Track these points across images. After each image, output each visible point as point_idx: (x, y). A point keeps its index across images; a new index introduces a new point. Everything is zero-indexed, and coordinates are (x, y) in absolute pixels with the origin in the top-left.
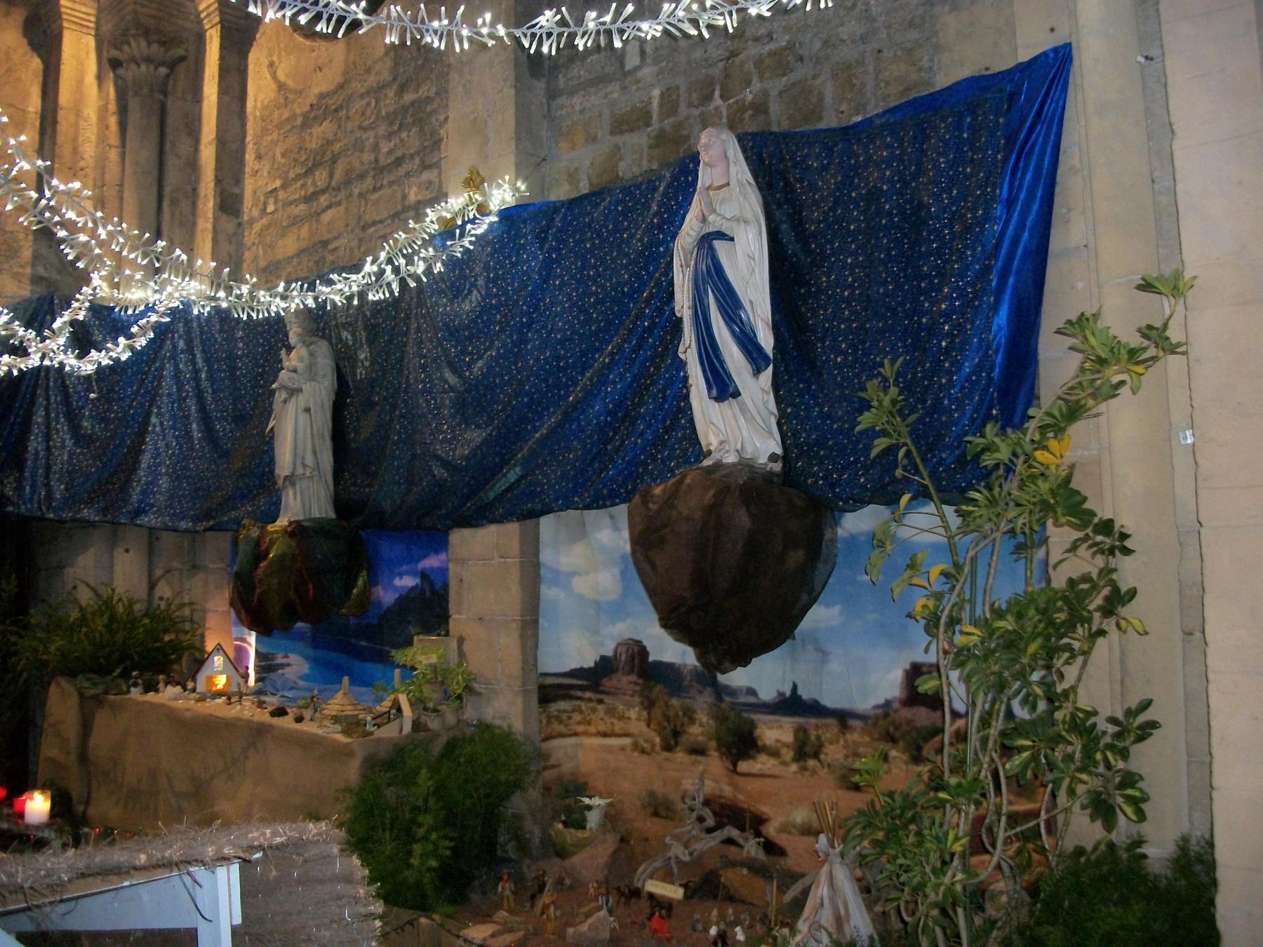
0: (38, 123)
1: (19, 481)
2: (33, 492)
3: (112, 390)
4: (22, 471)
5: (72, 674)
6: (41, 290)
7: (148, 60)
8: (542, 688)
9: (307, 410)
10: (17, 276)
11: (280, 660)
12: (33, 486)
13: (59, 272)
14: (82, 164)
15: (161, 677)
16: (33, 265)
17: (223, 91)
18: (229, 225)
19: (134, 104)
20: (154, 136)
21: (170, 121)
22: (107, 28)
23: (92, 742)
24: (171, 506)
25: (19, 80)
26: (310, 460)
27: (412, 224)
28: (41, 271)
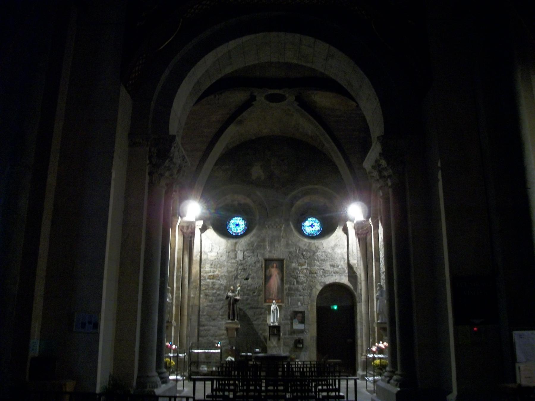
14: (354, 254)
18: (378, 264)
22: (356, 227)
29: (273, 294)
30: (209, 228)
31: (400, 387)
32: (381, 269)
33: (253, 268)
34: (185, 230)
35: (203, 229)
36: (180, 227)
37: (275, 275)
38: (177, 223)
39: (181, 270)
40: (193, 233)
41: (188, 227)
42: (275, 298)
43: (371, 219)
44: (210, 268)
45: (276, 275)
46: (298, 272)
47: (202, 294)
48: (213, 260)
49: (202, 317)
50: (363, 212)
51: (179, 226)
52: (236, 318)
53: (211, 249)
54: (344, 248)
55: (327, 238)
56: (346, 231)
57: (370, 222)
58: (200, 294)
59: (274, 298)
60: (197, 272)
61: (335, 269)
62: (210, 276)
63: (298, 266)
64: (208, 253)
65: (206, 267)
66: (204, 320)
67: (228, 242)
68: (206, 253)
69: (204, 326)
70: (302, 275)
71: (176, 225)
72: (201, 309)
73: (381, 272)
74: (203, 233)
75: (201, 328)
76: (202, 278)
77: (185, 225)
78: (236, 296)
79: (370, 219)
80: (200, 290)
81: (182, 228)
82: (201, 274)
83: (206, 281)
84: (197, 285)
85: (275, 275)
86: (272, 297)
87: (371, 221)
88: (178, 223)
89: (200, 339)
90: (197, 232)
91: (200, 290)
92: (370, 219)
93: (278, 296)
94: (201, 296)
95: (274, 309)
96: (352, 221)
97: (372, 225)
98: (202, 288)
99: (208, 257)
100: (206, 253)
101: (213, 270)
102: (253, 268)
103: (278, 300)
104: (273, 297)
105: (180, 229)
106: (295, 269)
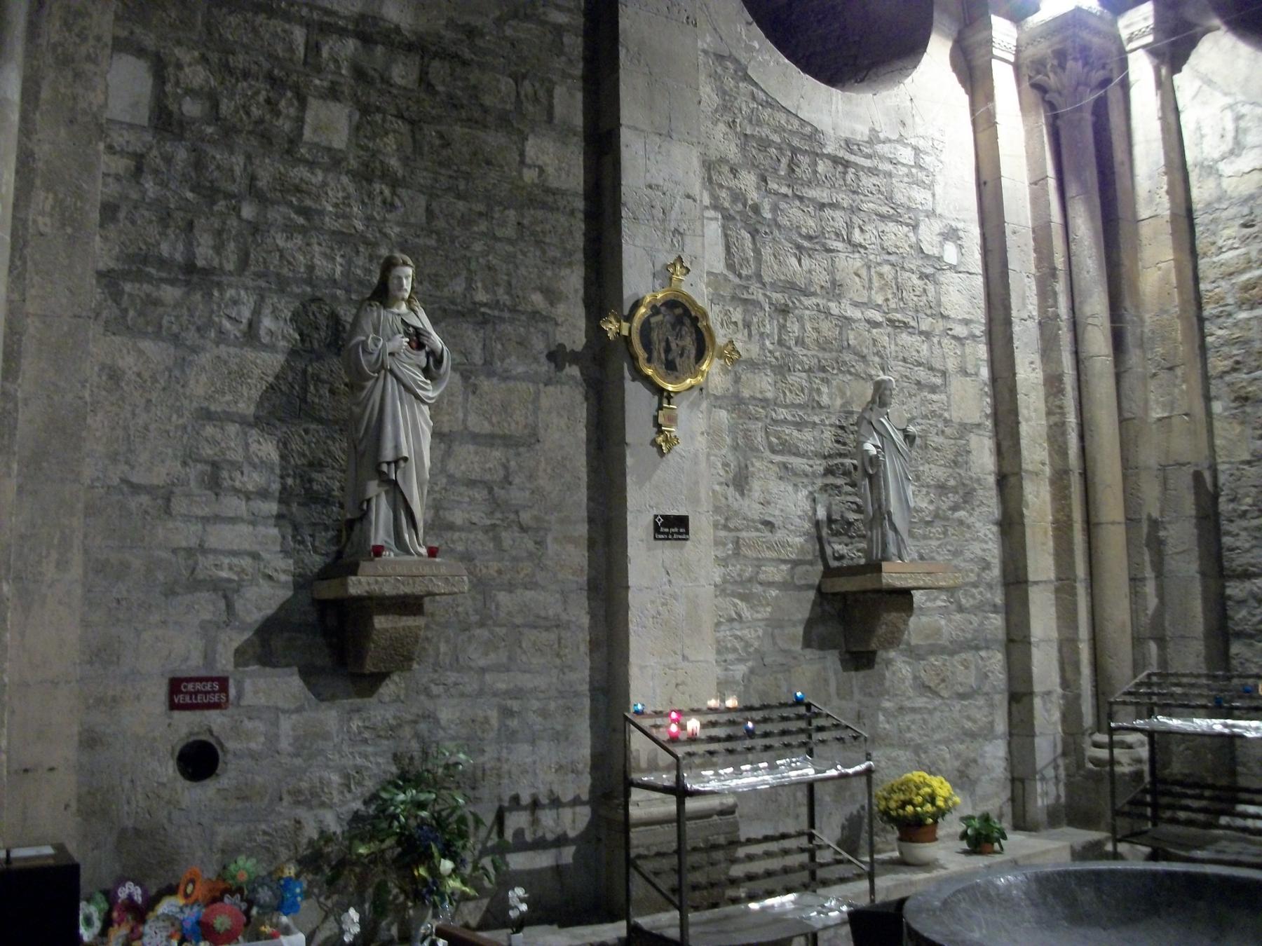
30: (1209, 30)
34: (1052, 81)
36: (1024, 70)
41: (1061, 56)
47: (1217, 398)
48: (1252, 197)
49: (1232, 528)
53: (1236, 138)
58: (1208, 399)
60: (1165, 280)
62: (1247, 287)
64: (1222, 166)
66: (1244, 541)
68: (1210, 169)
69: (1246, 575)
72: (1222, 479)
74: (1179, 70)
75: (1235, 589)
76: (1209, 310)
77: (1043, 49)
80: (1206, 378)
82: (1202, 286)
83: (1230, 320)
84: (1176, 348)
89: (1236, 648)
90: (1141, 70)
91: (1206, 378)
94: (1217, 407)
98: (1218, 364)
99: (1225, 183)
100: (1210, 169)
105: (1026, 84)
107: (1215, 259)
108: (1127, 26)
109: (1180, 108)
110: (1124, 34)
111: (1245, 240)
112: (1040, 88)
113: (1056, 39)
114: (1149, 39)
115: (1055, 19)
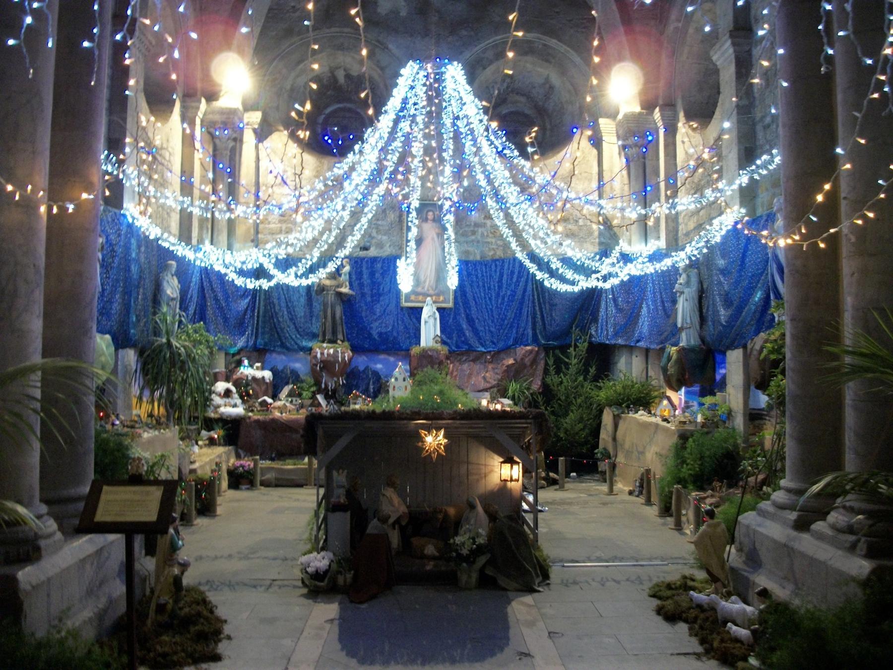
0: (597, 177)
1: (597, 327)
2: (601, 333)
3: (629, 290)
4: (597, 324)
5: (610, 406)
6: (603, 247)
7: (636, 145)
8: (751, 414)
9: (687, 300)
10: (592, 243)
11: (691, 404)
12: (602, 329)
13: (610, 239)
15: (641, 408)
16: (599, 238)
17: (666, 155)
19: (632, 165)
20: (641, 179)
21: (648, 170)
22: (620, 132)
23: (618, 433)
24: (650, 338)
25: (588, 161)
26: (689, 321)
27: (708, 227)
28: (602, 240)
29: (425, 282)
31: (870, 554)
32: (680, 228)
33: (380, 222)
35: (262, 134)
37: (430, 238)
38: (197, 114)
39: (210, 226)
40: (238, 140)
42: (431, 292)
43: (660, 111)
44: (280, 221)
45: (433, 239)
46: (485, 234)
50: (638, 98)
51: (202, 121)
52: (340, 336)
54: (590, 180)
55: (553, 156)
56: (597, 142)
57: (656, 118)
59: (428, 290)
61: (570, 226)
63: (484, 219)
65: (270, 220)
67: (320, 162)
70: (493, 240)
71: (195, 117)
73: (680, 234)
77: (217, 118)
78: (339, 286)
79: (657, 109)
81: (210, 127)
85: (430, 238)
86: (423, 288)
87: (659, 114)
88: (200, 114)
90: (249, 138)
92: (657, 109)
93: (436, 287)
95: (429, 317)
96: (613, 116)
97: (660, 124)
101: (286, 228)
102: (380, 222)
103: (438, 295)
104: (426, 289)
106: (477, 225)
107: (267, 226)
108: (248, 118)
109: (260, 158)
110: (245, 121)
111: (280, 221)
112: (212, 136)
113: (225, 116)
114: (256, 126)
115: (226, 108)
